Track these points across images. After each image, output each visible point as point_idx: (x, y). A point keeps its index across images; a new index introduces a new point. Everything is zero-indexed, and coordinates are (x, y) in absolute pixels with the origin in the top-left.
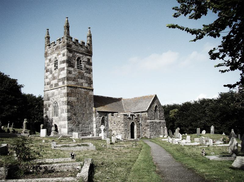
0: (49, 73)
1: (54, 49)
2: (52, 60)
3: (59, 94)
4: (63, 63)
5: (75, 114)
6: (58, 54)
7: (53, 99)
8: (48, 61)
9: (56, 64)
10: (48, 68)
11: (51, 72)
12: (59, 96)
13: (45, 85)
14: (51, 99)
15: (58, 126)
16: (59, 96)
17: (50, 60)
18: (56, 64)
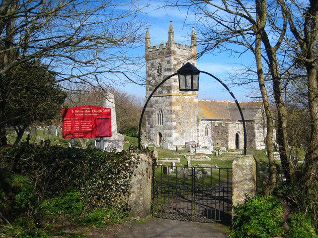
0: (151, 78)
1: (157, 54)
2: (155, 64)
3: (164, 101)
4: (168, 71)
5: (180, 123)
6: (162, 61)
7: (157, 107)
8: (150, 65)
9: (159, 71)
10: (150, 73)
11: (154, 78)
12: (164, 104)
13: (147, 90)
14: (154, 106)
15: (162, 134)
16: (164, 104)
17: (152, 64)
18: (159, 71)
